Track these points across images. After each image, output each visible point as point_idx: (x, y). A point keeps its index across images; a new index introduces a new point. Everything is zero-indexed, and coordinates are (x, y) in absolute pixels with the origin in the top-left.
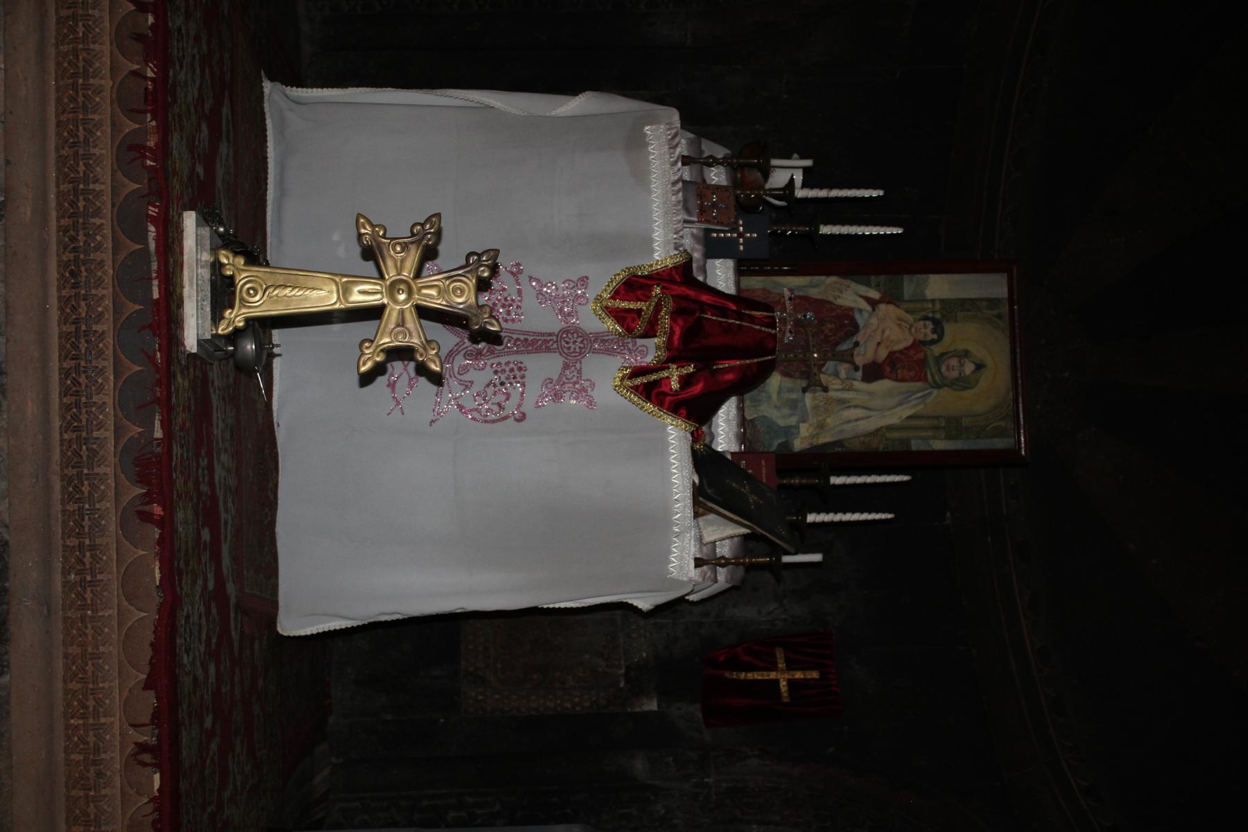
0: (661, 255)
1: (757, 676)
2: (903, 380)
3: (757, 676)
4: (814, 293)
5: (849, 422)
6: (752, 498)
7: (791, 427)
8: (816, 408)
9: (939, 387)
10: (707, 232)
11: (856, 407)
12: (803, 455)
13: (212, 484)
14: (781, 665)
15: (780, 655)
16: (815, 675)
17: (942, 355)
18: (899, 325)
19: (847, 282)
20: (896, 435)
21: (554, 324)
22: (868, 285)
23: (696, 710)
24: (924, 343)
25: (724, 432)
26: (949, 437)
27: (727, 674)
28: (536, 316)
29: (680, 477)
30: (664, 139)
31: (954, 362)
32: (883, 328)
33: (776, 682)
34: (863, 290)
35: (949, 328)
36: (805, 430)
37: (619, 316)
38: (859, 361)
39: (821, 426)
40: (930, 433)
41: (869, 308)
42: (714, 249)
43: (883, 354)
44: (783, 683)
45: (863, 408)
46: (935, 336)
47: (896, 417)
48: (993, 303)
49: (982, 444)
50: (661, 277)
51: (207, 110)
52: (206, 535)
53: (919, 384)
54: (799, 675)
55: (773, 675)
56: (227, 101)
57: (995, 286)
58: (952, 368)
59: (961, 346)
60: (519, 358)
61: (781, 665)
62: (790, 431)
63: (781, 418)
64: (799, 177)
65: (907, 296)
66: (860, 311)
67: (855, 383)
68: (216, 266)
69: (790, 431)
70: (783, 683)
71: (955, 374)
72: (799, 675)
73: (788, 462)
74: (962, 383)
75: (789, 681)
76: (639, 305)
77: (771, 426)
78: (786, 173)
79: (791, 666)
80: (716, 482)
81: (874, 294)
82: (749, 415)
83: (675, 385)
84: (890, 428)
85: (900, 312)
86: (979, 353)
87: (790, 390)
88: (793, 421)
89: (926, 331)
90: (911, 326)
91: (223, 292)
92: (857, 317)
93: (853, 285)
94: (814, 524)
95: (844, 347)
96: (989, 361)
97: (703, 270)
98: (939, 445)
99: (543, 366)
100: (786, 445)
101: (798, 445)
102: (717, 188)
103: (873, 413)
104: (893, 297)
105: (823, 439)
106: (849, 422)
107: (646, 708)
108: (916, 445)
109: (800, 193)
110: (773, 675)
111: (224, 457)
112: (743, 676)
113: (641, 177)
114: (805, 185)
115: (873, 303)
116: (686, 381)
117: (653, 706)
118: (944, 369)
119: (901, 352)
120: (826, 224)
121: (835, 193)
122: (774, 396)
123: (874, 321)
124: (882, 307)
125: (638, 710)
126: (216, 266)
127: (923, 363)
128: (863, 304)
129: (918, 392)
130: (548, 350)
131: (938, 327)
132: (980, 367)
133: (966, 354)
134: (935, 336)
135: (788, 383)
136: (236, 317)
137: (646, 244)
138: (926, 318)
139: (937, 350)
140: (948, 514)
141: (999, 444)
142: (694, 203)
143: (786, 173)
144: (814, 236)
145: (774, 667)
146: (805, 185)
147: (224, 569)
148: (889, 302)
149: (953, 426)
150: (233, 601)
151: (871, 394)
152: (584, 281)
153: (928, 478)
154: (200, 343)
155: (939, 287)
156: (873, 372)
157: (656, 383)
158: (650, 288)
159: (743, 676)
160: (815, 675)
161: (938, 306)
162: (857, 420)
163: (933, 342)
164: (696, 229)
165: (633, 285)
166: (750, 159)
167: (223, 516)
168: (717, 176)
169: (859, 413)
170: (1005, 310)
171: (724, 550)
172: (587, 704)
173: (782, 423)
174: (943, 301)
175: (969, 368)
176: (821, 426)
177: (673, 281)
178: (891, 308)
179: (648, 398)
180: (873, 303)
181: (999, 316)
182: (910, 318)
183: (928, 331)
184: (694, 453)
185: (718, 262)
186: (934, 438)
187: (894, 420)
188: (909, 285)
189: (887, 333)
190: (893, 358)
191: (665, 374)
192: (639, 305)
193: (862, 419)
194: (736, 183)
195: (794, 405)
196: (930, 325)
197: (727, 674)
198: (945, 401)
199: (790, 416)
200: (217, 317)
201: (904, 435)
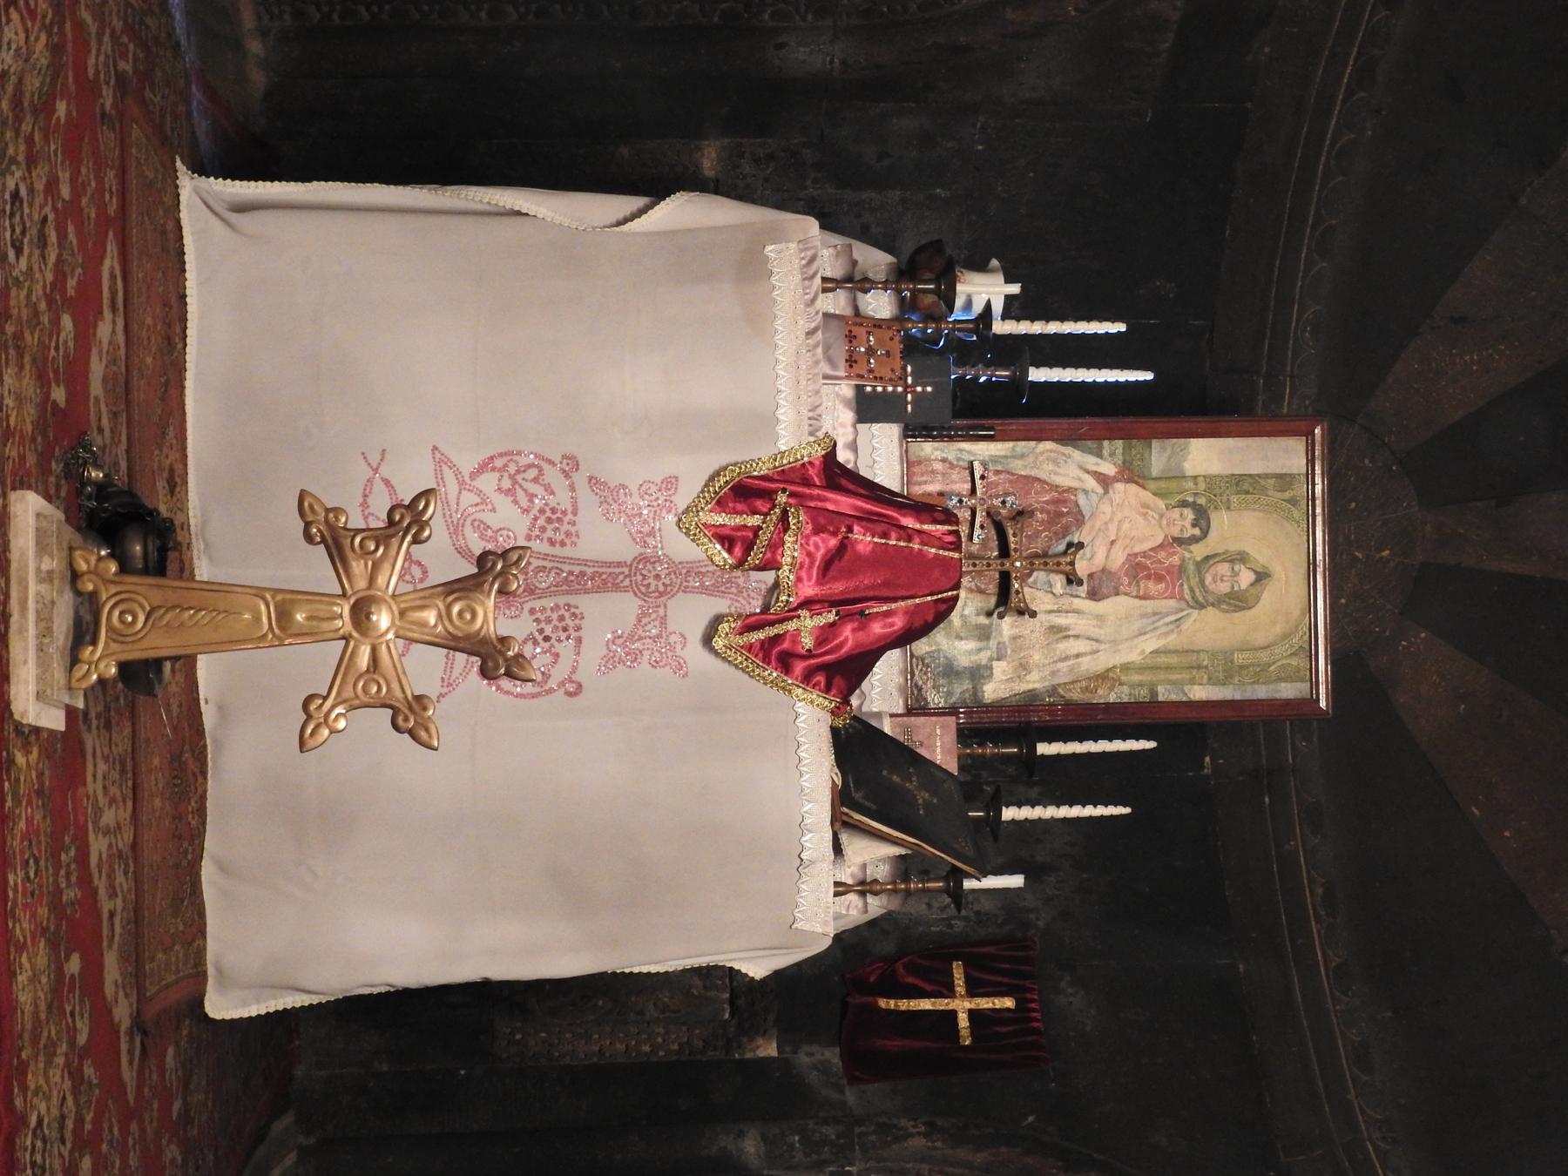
0: (789, 440)
1: (926, 1004)
3: (926, 1004)
4: (1019, 467)
5: (1067, 658)
6: (922, 796)
7: (979, 667)
9: (1202, 607)
10: (859, 389)
11: (1077, 637)
13: (85, 880)
14: (960, 987)
16: (1009, 1003)
17: (1207, 558)
18: (1145, 515)
19: (1068, 450)
20: (1136, 678)
21: (626, 551)
23: (832, 1055)
24: (1179, 541)
25: (881, 693)
26: (1212, 681)
27: (882, 1003)
28: (601, 538)
29: (816, 773)
30: (797, 263)
31: (1224, 569)
33: (954, 1013)
34: (1091, 462)
35: (1220, 521)
36: (999, 668)
37: (726, 539)
38: (1082, 567)
39: (1024, 667)
40: (1186, 676)
41: (1100, 490)
42: (869, 409)
43: (1118, 558)
44: (963, 1021)
45: (1089, 638)
46: (1197, 531)
47: (1134, 652)
48: (1284, 480)
49: (1262, 692)
50: (793, 476)
51: (71, 292)
52: (74, 965)
53: (1172, 603)
54: (985, 1003)
56: (112, 248)
57: (1284, 455)
58: (1220, 580)
59: (1234, 547)
60: (572, 599)
61: (960, 987)
62: (978, 674)
64: (998, 308)
65: (1156, 470)
66: (1086, 492)
67: (1076, 601)
69: (978, 674)
70: (963, 1021)
71: (1224, 588)
72: (985, 1003)
74: (1237, 601)
75: (971, 1012)
76: (754, 521)
77: (950, 671)
78: (983, 291)
79: (972, 993)
80: (870, 772)
81: (1108, 469)
83: (807, 642)
84: (1126, 668)
85: (1147, 496)
86: (1261, 555)
88: (983, 657)
89: (1183, 522)
90: (1161, 516)
92: (1082, 500)
93: (1077, 455)
96: (1277, 569)
97: (853, 447)
98: (1199, 693)
99: (608, 615)
100: (976, 692)
101: (992, 691)
102: (878, 324)
103: (1103, 647)
104: (1132, 474)
105: (1024, 687)
106: (1067, 658)
107: (761, 1053)
108: (1164, 694)
109: (1000, 327)
111: (108, 818)
112: (904, 1005)
113: (758, 321)
114: (1006, 316)
115: (1104, 481)
116: (825, 635)
117: (769, 1049)
118: (1208, 579)
119: (1144, 554)
121: (1053, 328)
123: (1106, 508)
124: (1119, 486)
125: (749, 1055)
128: (1091, 483)
129: (1167, 614)
130: (617, 588)
131: (1202, 518)
132: (1262, 576)
133: (1242, 558)
134: (1197, 531)
137: (766, 423)
138: (1184, 504)
139: (1199, 551)
140: (1207, 759)
141: (1288, 691)
142: (840, 351)
144: (1018, 384)
145: (949, 992)
147: (109, 989)
148: (1130, 480)
149: (1227, 668)
150: (125, 1024)
151: (1100, 619)
152: (671, 483)
153: (1187, 757)
155: (1206, 456)
157: (777, 639)
158: (769, 495)
159: (904, 1005)
160: (1009, 1003)
161: (1202, 486)
162: (1077, 656)
163: (1195, 540)
164: (847, 389)
165: (745, 492)
166: (926, 270)
167: (106, 906)
168: (880, 305)
170: (1301, 490)
171: (882, 872)
172: (676, 1047)
173: (964, 662)
175: (1246, 578)
177: (807, 482)
178: (1133, 488)
179: (766, 660)
180: (1104, 481)
181: (1293, 502)
182: (1161, 504)
183: (1188, 523)
184: (834, 731)
185: (876, 428)
186: (1192, 682)
187: (1134, 657)
188: (1159, 455)
189: (1126, 526)
191: (791, 626)
192: (754, 521)
193: (1085, 654)
194: (906, 307)
195: (984, 634)
196: (1189, 515)
197: (882, 1003)
198: (1208, 629)
199: (980, 650)
201: (1146, 677)
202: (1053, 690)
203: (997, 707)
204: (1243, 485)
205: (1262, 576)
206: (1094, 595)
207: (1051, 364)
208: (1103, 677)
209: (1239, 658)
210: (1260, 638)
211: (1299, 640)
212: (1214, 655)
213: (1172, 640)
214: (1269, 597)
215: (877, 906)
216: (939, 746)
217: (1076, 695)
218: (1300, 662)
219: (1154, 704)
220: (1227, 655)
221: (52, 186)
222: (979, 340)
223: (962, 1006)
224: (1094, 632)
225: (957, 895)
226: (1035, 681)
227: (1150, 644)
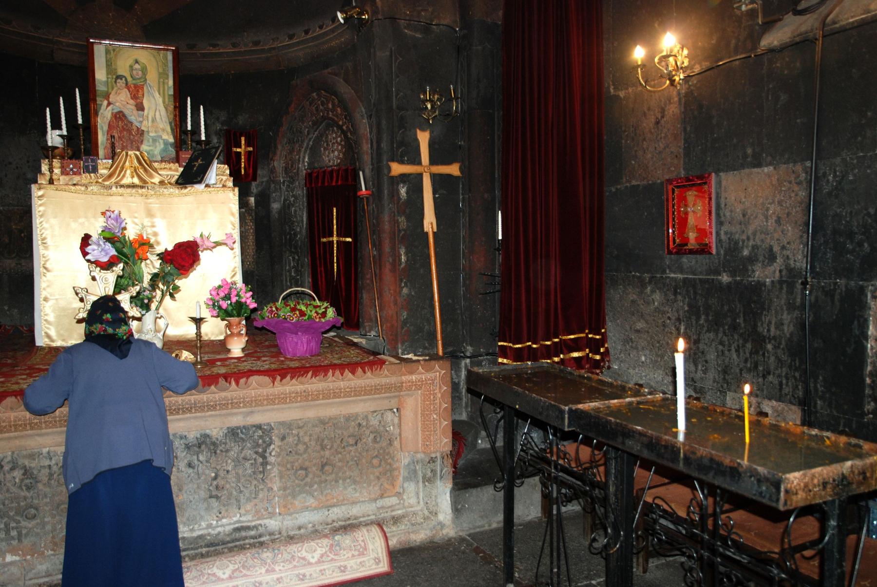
2: (143, 95)
4: (106, 128)
8: (156, 132)
12: (175, 137)
20: (167, 100)
22: (101, 105)
24: (127, 84)
26: (167, 78)
31: (135, 72)
32: (121, 100)
35: (120, 72)
36: (165, 137)
39: (163, 130)
43: (132, 102)
47: (160, 100)
48: (107, 52)
49: (170, 65)
59: (128, 68)
62: (166, 143)
63: (160, 146)
64: (58, 132)
69: (166, 143)
71: (140, 72)
73: (179, 144)
74: (144, 70)
77: (165, 150)
81: (105, 103)
82: (159, 158)
84: (164, 102)
85: (113, 93)
86: (131, 61)
87: (148, 141)
88: (161, 141)
89: (121, 83)
92: (115, 111)
94: (206, 136)
96: (135, 57)
98: (171, 83)
100: (171, 145)
101: (171, 140)
104: (107, 96)
105: (169, 130)
108: (171, 92)
114: (60, 129)
115: (109, 104)
120: (77, 120)
122: (151, 148)
127: (136, 86)
128: (110, 108)
131: (119, 77)
132: (137, 62)
133: (131, 67)
135: (145, 142)
138: (116, 82)
139: (129, 79)
141: (170, 56)
143: (54, 138)
146: (60, 129)
149: (163, 75)
151: (149, 109)
155: (100, 74)
156: (140, 107)
163: (126, 80)
169: (157, 113)
174: (108, 74)
175: (137, 66)
176: (163, 130)
180: (109, 104)
182: (115, 89)
188: (100, 87)
190: (134, 97)
195: (155, 140)
196: (119, 81)
198: (152, 76)
202: (170, 123)
204: (109, 65)
205: (137, 62)
207: (77, 117)
208: (166, 109)
209: (161, 70)
210: (155, 64)
211: (155, 52)
212: (160, 78)
213: (156, 89)
214: (143, 60)
216: (186, 156)
217: (172, 116)
219: (175, 96)
220: (160, 74)
221: (24, 379)
222: (68, 139)
224: (154, 109)
226: (169, 129)
227: (157, 95)
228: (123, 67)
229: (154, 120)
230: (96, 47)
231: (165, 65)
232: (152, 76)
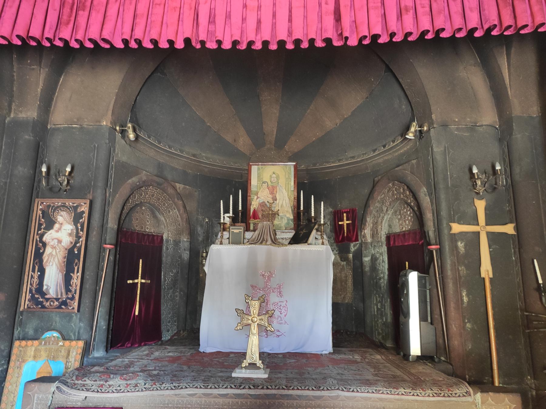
15: (340, 223)
16: (345, 214)
31: (272, 179)
33: (347, 224)
35: (264, 180)
36: (288, 215)
38: (272, 202)
39: (287, 212)
43: (271, 196)
44: (348, 222)
48: (259, 169)
54: (345, 218)
55: (345, 225)
57: (254, 169)
58: (274, 180)
62: (288, 219)
63: (285, 221)
68: (246, 368)
70: (348, 222)
72: (345, 218)
74: (278, 177)
77: (288, 223)
81: (256, 197)
84: (288, 195)
86: (271, 173)
88: (286, 218)
89: (265, 185)
91: (253, 366)
95: (268, 204)
98: (292, 183)
100: (291, 220)
101: (292, 217)
104: (257, 194)
108: (293, 189)
109: (231, 214)
110: (345, 225)
115: (258, 198)
124: (259, 196)
126: (246, 368)
128: (258, 200)
131: (264, 183)
132: (274, 173)
133: (271, 176)
135: (276, 219)
136: (259, 363)
139: (269, 183)
141: (293, 169)
143: (226, 218)
149: (288, 179)
154: (265, 373)
155: (254, 181)
169: (284, 202)
170: (260, 166)
173: (286, 221)
175: (274, 176)
180: (258, 198)
187: (286, 194)
190: (272, 193)
195: (282, 218)
196: (264, 184)
198: (282, 181)
200: (259, 368)
202: (291, 207)
203: (294, 217)
204: (259, 176)
205: (274, 173)
206: (276, 200)
208: (289, 199)
209: (287, 177)
215: (325, 236)
218: (288, 167)
223: (346, 222)
225: (324, 224)
228: (266, 177)
229: (282, 206)
230: (253, 167)
231: (290, 173)
232: (282, 181)
